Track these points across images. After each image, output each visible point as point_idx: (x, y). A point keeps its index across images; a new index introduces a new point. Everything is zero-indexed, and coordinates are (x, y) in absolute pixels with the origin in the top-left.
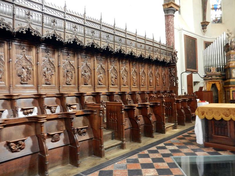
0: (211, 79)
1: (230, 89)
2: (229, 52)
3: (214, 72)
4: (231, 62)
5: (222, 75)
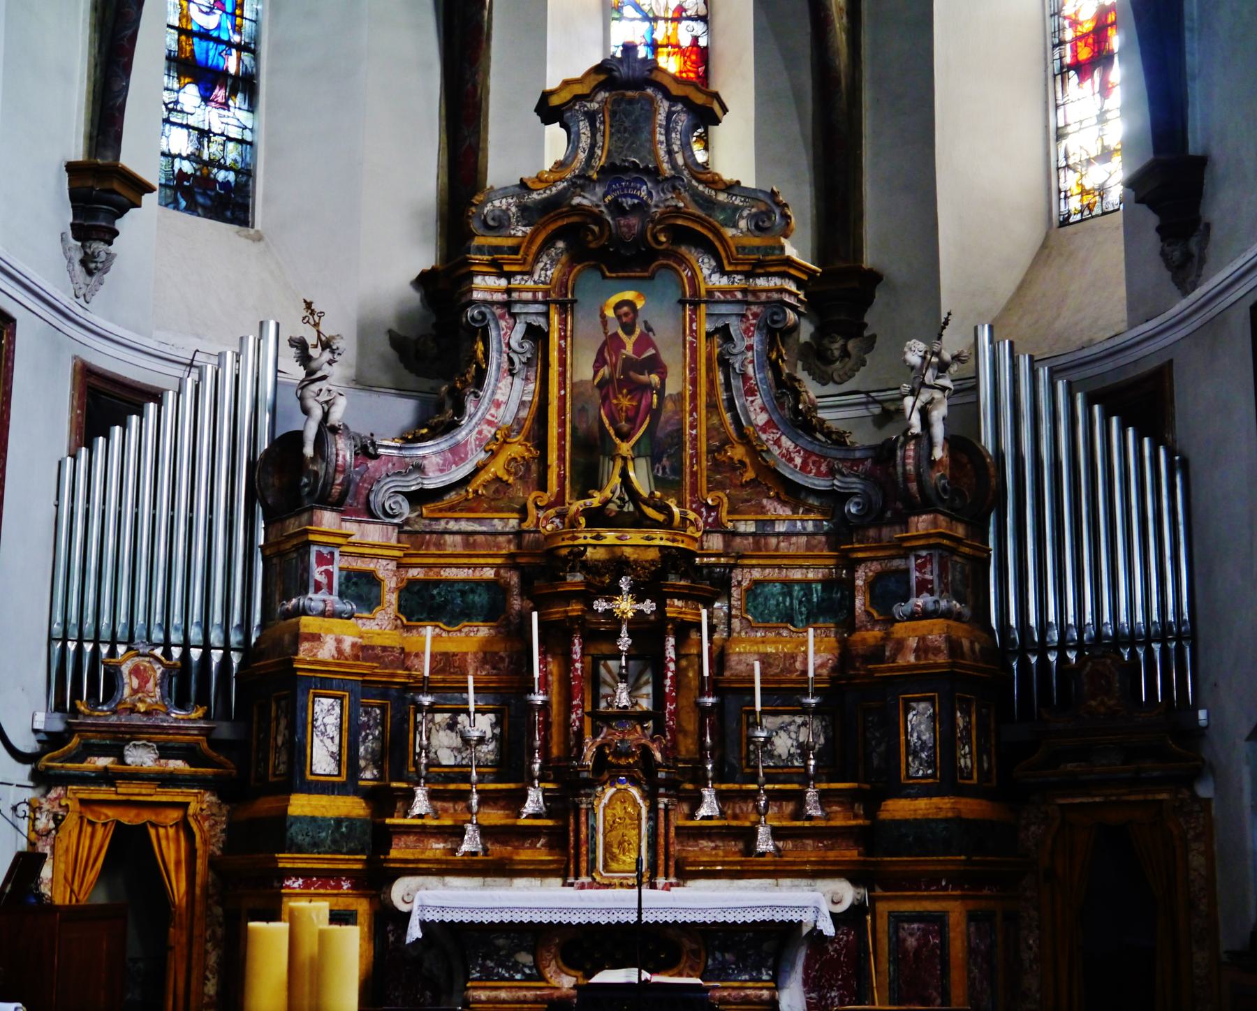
0: (106, 777)
1: (281, 896)
2: (292, 526)
3: (142, 707)
4: (308, 624)
5: (213, 744)
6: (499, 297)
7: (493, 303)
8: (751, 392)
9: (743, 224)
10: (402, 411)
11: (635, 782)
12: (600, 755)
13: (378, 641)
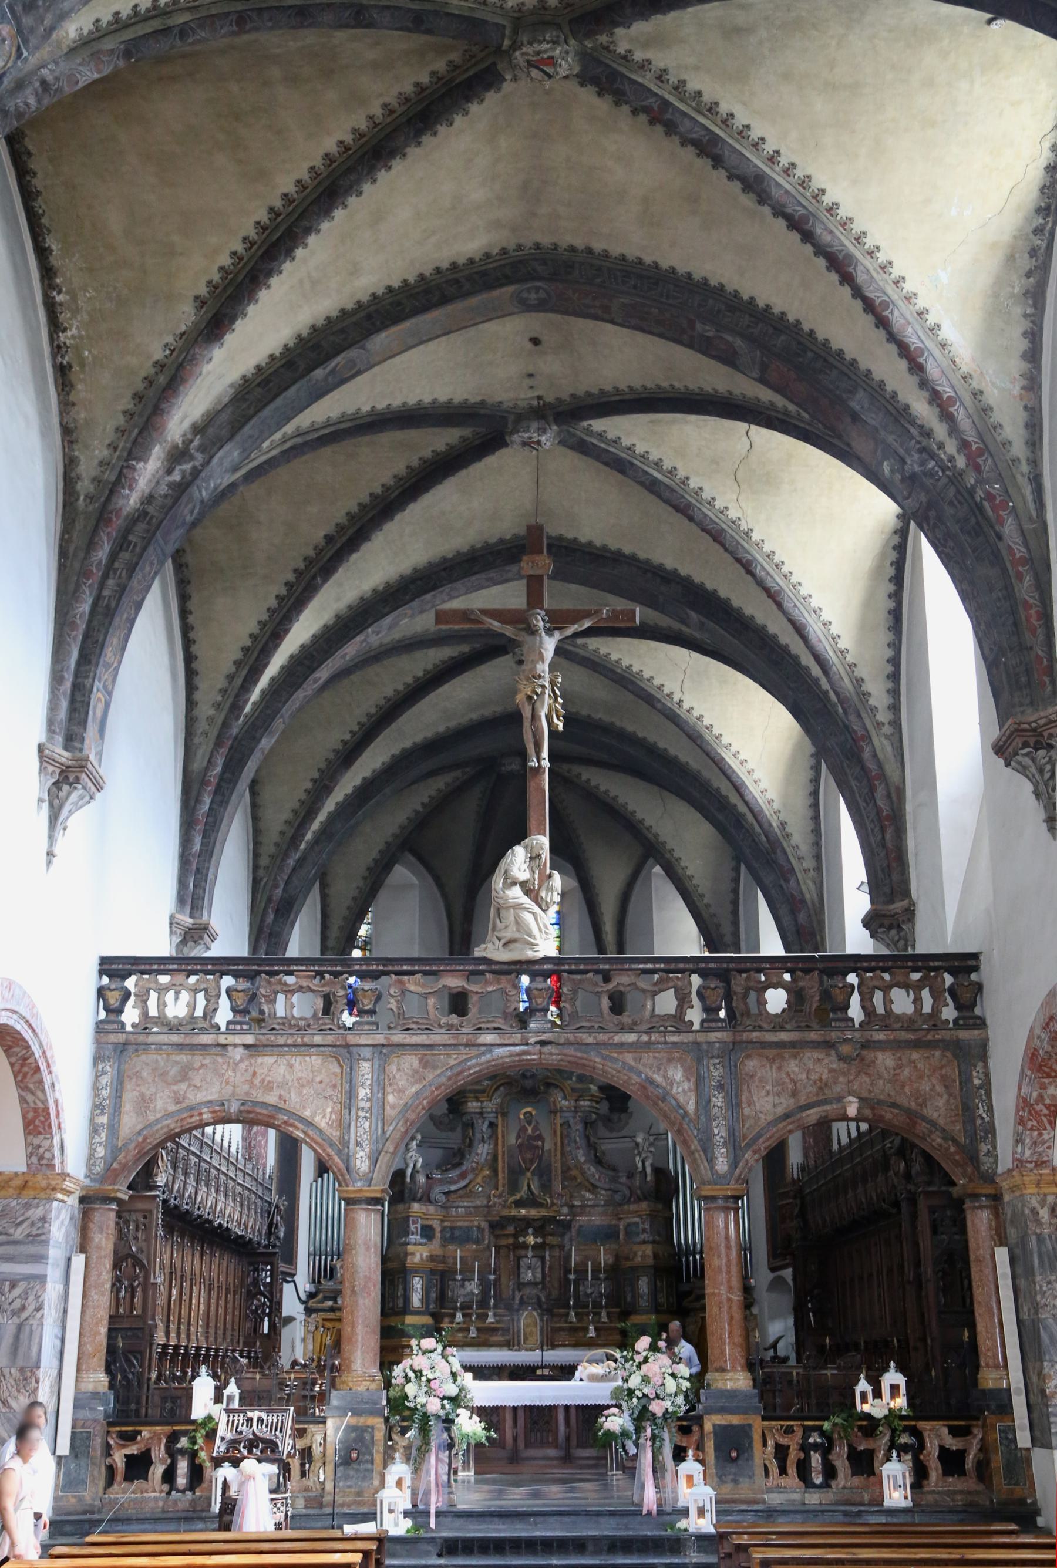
2: (400, 1207)
4: (410, 1248)
6: (478, 1110)
7: (475, 1113)
8: (578, 1148)
9: (574, 1079)
10: (437, 1154)
11: (535, 1309)
12: (522, 1298)
13: (434, 1253)
